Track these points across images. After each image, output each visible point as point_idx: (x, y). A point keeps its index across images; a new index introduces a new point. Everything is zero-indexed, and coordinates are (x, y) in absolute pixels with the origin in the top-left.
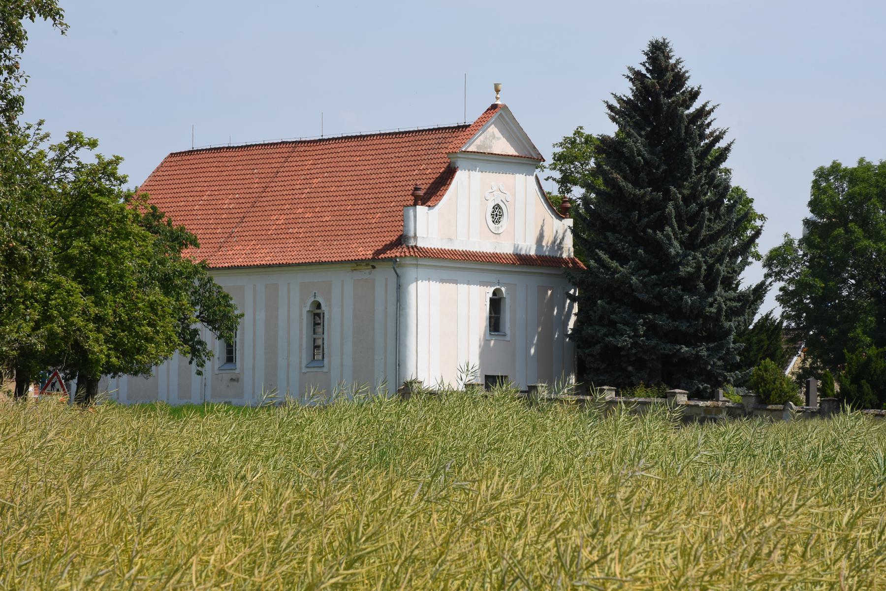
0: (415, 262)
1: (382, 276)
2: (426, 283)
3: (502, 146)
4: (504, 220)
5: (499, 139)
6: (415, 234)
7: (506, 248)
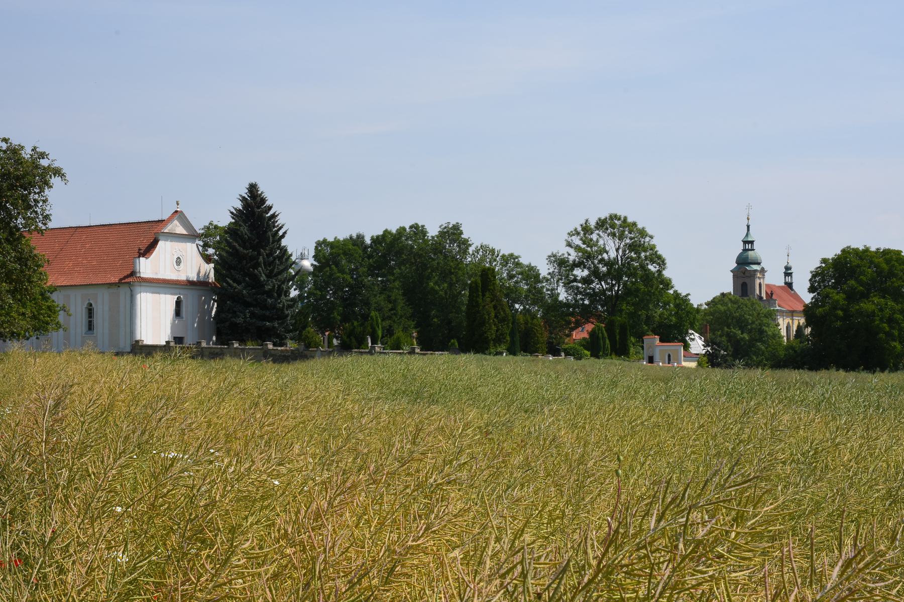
1: (123, 291)
3: (180, 230)
4: (182, 264)
7: (183, 277)
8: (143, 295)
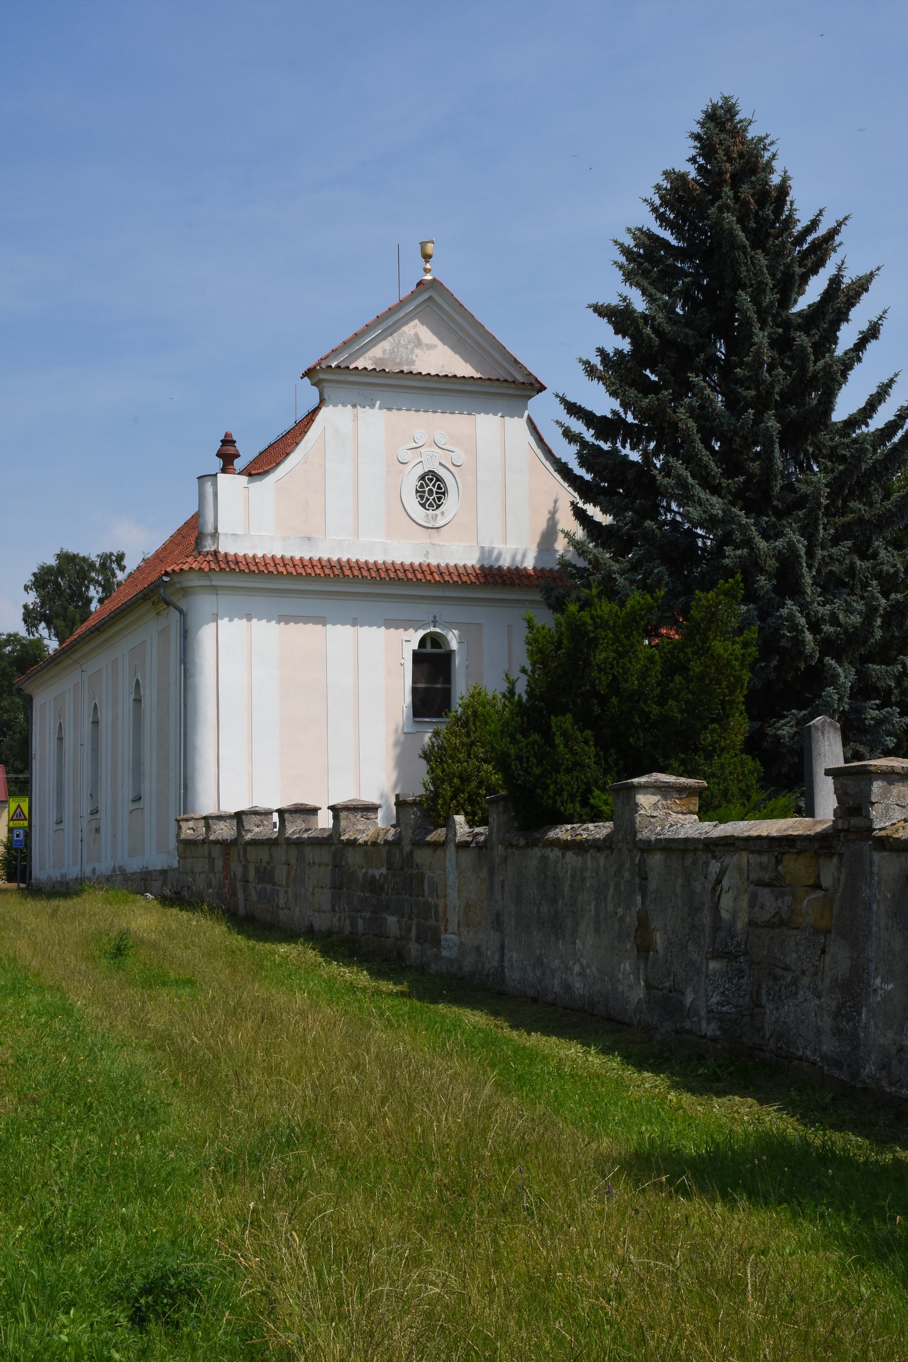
0: (208, 583)
2: (240, 624)
3: (438, 358)
4: (450, 503)
5: (430, 347)
6: (216, 528)
8: (223, 623)
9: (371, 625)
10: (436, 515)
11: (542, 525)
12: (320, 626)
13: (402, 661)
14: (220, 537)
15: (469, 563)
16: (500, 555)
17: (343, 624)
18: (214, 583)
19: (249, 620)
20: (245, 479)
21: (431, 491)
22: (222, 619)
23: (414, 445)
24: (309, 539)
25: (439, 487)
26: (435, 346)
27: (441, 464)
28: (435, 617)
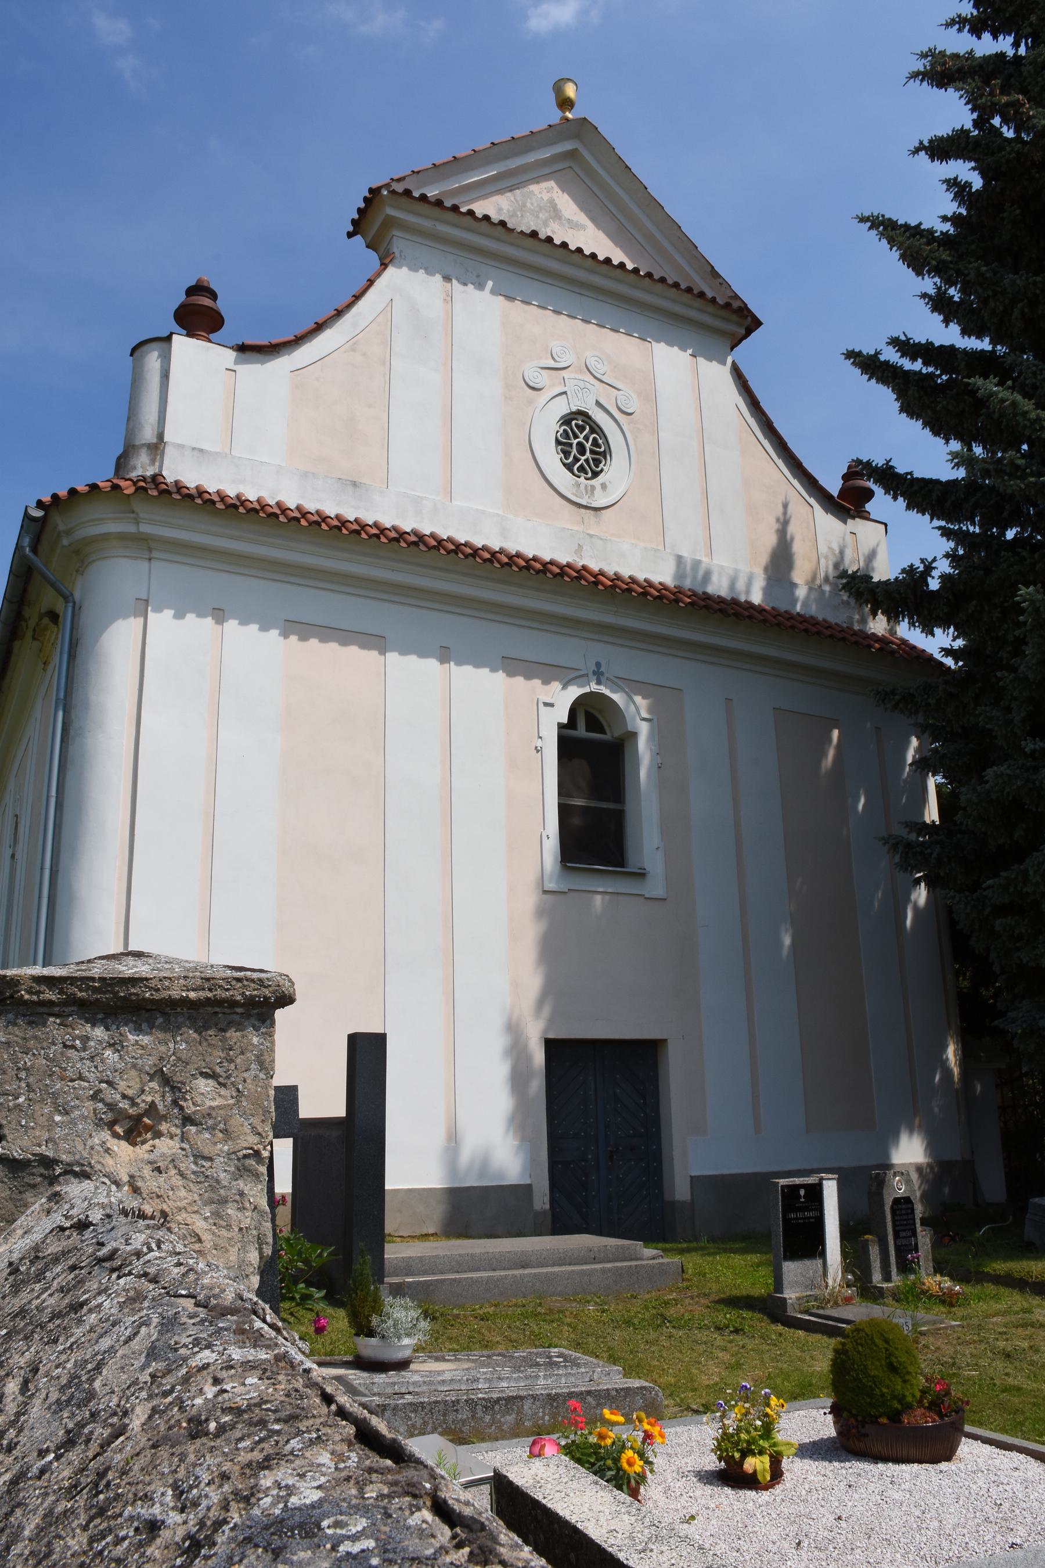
0: (131, 528)
2: (198, 627)
6: (161, 436)
8: (161, 622)
9: (477, 666)
10: (593, 488)
11: (771, 540)
12: (374, 653)
13: (539, 743)
14: (169, 452)
15: (656, 579)
16: (707, 576)
17: (423, 654)
18: (145, 528)
19: (220, 620)
20: (231, 355)
21: (581, 449)
22: (158, 610)
23: (552, 364)
24: (355, 484)
25: (595, 443)
26: (583, 227)
27: (598, 404)
28: (598, 665)
